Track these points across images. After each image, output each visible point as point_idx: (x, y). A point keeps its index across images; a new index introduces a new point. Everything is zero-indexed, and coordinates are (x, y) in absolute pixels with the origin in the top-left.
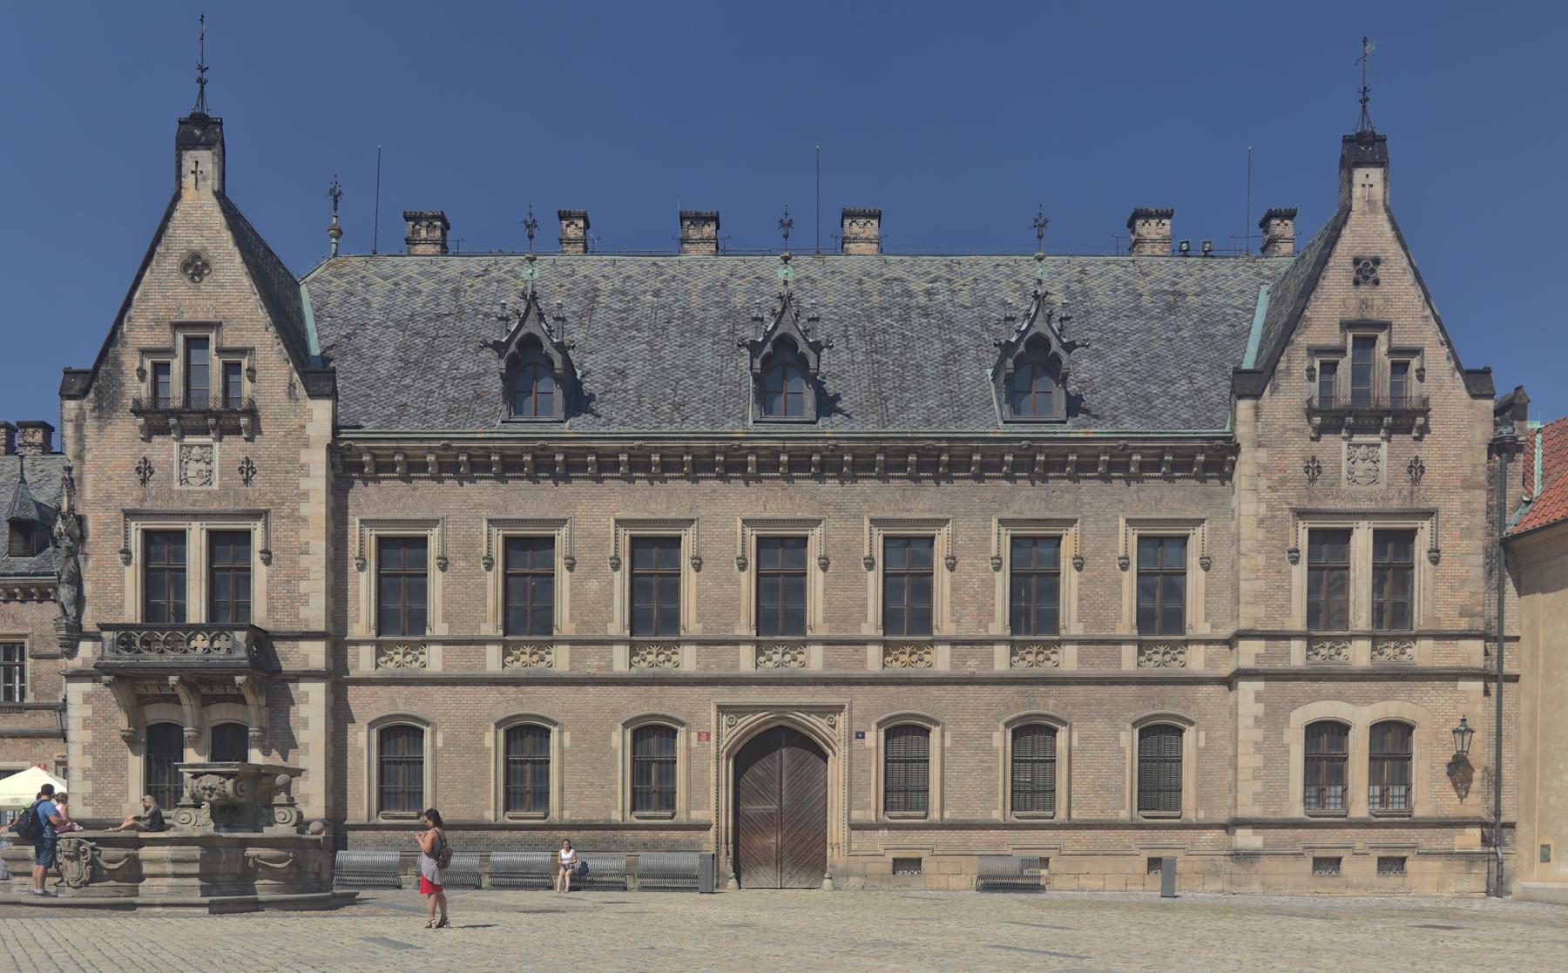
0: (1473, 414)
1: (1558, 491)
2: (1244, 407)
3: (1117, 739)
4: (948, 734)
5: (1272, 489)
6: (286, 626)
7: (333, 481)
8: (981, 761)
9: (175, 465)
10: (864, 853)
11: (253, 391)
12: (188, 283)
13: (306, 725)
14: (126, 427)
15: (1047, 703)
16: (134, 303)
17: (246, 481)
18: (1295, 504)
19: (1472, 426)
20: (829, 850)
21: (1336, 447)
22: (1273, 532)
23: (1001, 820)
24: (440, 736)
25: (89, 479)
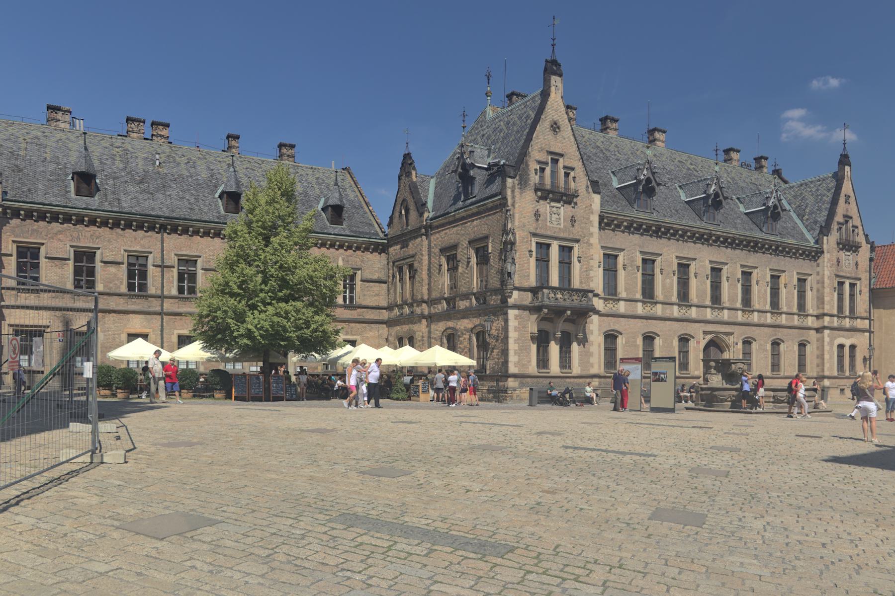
5: (831, 267)
13: (592, 334)
14: (530, 195)
17: (573, 225)
21: (843, 255)
25: (517, 216)
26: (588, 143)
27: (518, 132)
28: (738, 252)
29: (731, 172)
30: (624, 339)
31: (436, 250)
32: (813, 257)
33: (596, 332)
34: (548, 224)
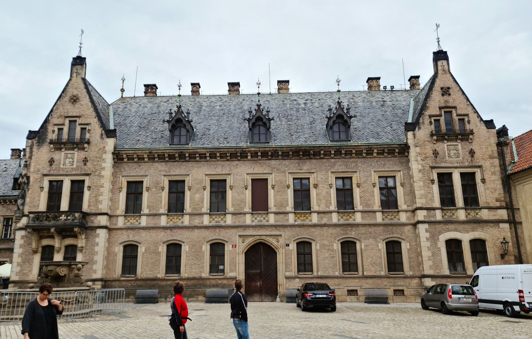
0: (489, 134)
1: (524, 159)
2: (410, 134)
3: (378, 246)
4: (318, 244)
5: (423, 160)
6: (94, 211)
7: (113, 164)
8: (330, 254)
9: (62, 159)
10: (291, 288)
11: (89, 136)
12: (72, 105)
15: (352, 234)
16: (54, 111)
17: (85, 164)
18: (431, 165)
19: (490, 138)
20: (278, 287)
21: (443, 147)
22: (425, 174)
23: (339, 275)
25: (33, 165)
28: (287, 162)
34: (62, 166)
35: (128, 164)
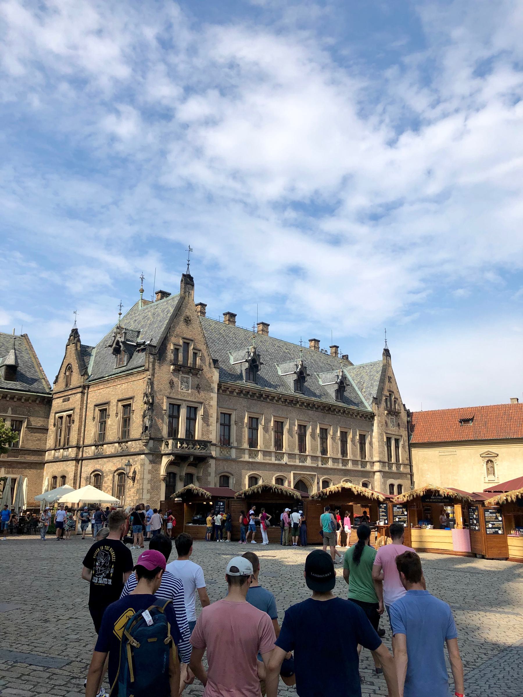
24: (235, 479)
26: (213, 331)
27: (160, 321)
28: (317, 414)
29: (314, 355)
30: (235, 479)
31: (91, 406)
32: (369, 419)
33: (213, 474)
34: (180, 390)
35: (222, 395)
